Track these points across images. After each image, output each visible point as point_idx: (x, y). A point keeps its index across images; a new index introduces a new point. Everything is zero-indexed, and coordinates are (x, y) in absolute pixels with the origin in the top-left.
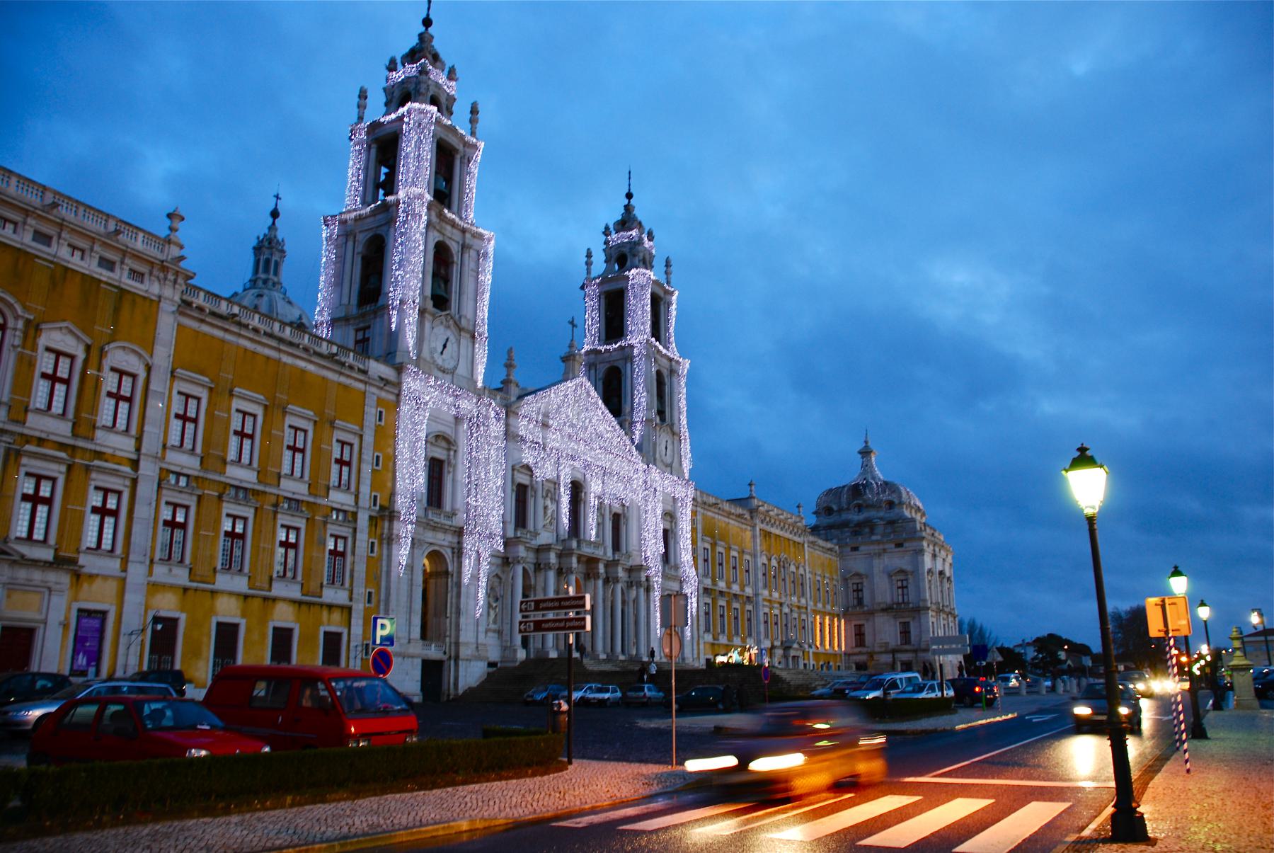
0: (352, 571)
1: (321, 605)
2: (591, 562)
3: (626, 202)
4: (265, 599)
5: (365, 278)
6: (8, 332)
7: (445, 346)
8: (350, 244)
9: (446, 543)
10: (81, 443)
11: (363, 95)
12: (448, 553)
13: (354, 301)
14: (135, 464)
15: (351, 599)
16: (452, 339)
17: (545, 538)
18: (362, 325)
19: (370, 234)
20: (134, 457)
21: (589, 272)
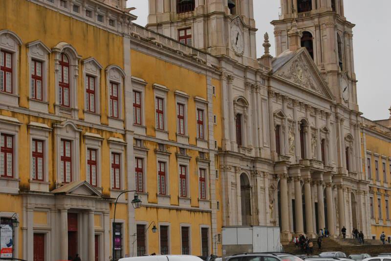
0: (210, 189)
1: (199, 211)
2: (316, 173)
4: (177, 210)
6: (72, 68)
7: (237, 39)
9: (248, 168)
10: (104, 128)
12: (248, 174)
13: (175, 11)
14: (124, 136)
15: (211, 208)
16: (240, 33)
17: (292, 161)
18: (184, 27)
20: (123, 132)
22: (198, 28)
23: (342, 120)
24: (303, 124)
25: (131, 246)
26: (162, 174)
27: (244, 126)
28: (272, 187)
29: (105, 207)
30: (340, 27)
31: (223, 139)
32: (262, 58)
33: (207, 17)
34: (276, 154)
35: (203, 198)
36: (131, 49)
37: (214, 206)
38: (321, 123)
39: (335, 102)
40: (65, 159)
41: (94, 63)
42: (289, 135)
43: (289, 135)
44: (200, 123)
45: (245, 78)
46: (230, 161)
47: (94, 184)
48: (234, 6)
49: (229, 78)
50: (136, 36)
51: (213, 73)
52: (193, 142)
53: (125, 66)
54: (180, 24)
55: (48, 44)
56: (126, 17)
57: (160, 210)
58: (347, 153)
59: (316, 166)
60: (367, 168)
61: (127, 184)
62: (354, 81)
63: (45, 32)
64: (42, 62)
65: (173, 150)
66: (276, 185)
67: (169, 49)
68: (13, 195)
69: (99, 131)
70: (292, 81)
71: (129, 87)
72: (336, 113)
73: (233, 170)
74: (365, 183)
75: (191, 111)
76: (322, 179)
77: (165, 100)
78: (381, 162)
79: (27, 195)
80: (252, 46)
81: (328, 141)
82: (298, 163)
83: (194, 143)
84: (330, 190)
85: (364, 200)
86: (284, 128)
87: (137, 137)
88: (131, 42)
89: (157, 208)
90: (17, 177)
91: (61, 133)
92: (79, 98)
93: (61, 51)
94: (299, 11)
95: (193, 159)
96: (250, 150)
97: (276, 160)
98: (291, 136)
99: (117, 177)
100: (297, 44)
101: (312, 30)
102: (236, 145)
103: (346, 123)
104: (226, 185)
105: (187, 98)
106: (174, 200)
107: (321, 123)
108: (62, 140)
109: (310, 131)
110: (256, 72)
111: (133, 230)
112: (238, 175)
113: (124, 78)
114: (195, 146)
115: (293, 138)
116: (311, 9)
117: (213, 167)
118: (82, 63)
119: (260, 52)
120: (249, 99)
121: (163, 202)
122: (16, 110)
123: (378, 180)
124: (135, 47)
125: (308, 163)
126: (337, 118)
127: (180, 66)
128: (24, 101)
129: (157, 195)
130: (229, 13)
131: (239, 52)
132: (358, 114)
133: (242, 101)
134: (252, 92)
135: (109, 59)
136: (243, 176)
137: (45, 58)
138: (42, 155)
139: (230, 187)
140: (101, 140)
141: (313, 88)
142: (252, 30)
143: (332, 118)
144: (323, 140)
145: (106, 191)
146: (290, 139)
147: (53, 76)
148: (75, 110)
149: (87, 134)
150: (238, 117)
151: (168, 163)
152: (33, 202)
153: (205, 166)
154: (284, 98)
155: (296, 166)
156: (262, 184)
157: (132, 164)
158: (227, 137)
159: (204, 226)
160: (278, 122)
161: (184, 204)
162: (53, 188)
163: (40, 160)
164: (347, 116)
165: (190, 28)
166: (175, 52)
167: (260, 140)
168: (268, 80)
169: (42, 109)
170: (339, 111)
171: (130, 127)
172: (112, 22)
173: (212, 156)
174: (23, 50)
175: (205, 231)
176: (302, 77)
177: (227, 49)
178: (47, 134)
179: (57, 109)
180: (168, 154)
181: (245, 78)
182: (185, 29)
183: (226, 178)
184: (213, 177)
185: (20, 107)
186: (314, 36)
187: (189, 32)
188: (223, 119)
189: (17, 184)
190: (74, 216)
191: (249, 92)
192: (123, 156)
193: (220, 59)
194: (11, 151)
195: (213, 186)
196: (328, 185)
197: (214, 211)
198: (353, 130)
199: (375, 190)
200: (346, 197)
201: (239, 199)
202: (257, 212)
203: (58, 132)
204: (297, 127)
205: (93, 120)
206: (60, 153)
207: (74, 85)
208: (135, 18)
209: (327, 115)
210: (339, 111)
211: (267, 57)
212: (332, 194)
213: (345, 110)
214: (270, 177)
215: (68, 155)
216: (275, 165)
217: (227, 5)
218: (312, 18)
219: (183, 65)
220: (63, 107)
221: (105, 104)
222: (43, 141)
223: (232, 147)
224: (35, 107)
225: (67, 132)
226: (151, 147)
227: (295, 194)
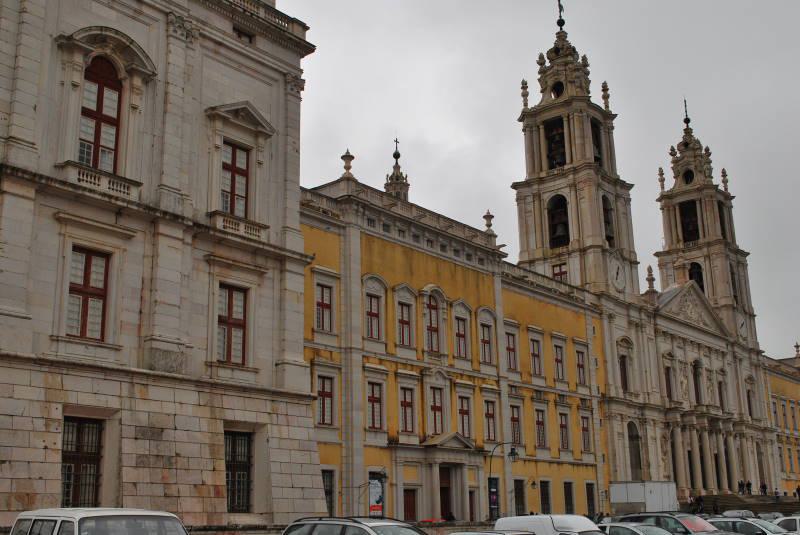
1: (583, 465)
2: (714, 420)
3: (685, 126)
4: (559, 463)
5: (553, 228)
6: (441, 311)
8: (537, 203)
10: (475, 375)
11: (524, 86)
13: (548, 246)
14: (498, 382)
16: (621, 267)
17: (686, 407)
18: (558, 263)
19: (554, 194)
21: (663, 187)
22: (573, 265)
23: (741, 360)
24: (696, 365)
25: (508, 503)
26: (540, 424)
27: (629, 370)
28: (664, 437)
29: (479, 460)
30: (732, 256)
31: (607, 384)
32: (647, 293)
33: (583, 251)
34: (667, 399)
35: (586, 450)
36: (503, 288)
37: (600, 459)
38: (717, 364)
39: (732, 340)
40: (435, 408)
41: (463, 305)
42: (680, 378)
43: (680, 378)
44: (580, 366)
45: (628, 316)
46: (615, 408)
47: (467, 435)
48: (612, 238)
49: (611, 317)
50: (507, 275)
51: (592, 311)
52: (573, 388)
53: (497, 307)
54: (553, 260)
55: (415, 289)
56: (496, 255)
57: (539, 464)
58: (749, 397)
59: (713, 412)
60: (773, 414)
61: (502, 434)
62: (752, 316)
63: (412, 274)
64: (409, 306)
65: (551, 397)
66: (669, 435)
67: (543, 287)
68: (381, 448)
69: (470, 377)
70: (681, 317)
71: (502, 330)
72: (734, 352)
73: (619, 418)
74: (772, 431)
75: (570, 352)
76: (721, 427)
77: (541, 343)
78: (789, 406)
79: (396, 449)
80: (634, 281)
81: (726, 384)
82: (693, 409)
83: (574, 389)
84: (731, 439)
85: (772, 451)
86: (675, 370)
87: (511, 383)
88: (503, 281)
89: (536, 461)
90: (385, 429)
91: (430, 381)
92: (448, 343)
93: (429, 293)
94: (686, 240)
95: (574, 407)
96: (637, 396)
97: (668, 406)
98: (683, 378)
99: (491, 428)
100: (684, 275)
101: (700, 261)
102: (621, 391)
103: (746, 363)
104: (612, 435)
105: (565, 340)
106: (555, 451)
107: (717, 364)
108: (431, 388)
109: (704, 373)
110: (640, 309)
111: (511, 486)
112: (625, 424)
113: (495, 320)
114: (575, 392)
115: (685, 381)
116: (698, 238)
117: (597, 415)
118: (451, 305)
119: (644, 287)
120: (633, 338)
121: (542, 455)
122: (383, 357)
123: (786, 427)
124: (506, 286)
125: (705, 409)
126: (735, 357)
127: (556, 305)
128: (391, 349)
129: (535, 447)
130: (607, 246)
131: (620, 288)
132: (759, 353)
133: (626, 341)
134: (637, 331)
135: (478, 300)
136: (631, 426)
137: (412, 301)
138: (410, 405)
139: (616, 437)
140: (473, 388)
141: (705, 324)
142: (634, 263)
143: (729, 358)
144: (720, 383)
145: (480, 443)
146: (683, 383)
147: (421, 321)
148: (444, 355)
149: (458, 381)
150: (623, 359)
151: (546, 412)
152: (402, 455)
153: (587, 414)
154: (673, 337)
155: (691, 413)
156: (653, 434)
157: (507, 413)
158: (611, 381)
159: (590, 482)
160: (668, 364)
161: (566, 457)
162: (423, 439)
163: (409, 410)
164: (746, 355)
165: (565, 264)
166: (550, 290)
167: (647, 383)
168: (655, 317)
169: (411, 355)
170: (736, 349)
171: (503, 372)
172: (481, 261)
173: (595, 402)
174: (390, 294)
175: (590, 487)
176: (693, 313)
177: (607, 285)
178: (416, 383)
179: (426, 355)
180: (547, 402)
181: (628, 316)
182: (560, 266)
183: (612, 428)
184: (597, 426)
185: (388, 354)
186: (703, 267)
187: (564, 269)
188: (605, 362)
189: (386, 436)
190: (447, 470)
191: (633, 331)
192: (497, 404)
193: (599, 296)
194: (379, 400)
195: (597, 435)
196: (728, 433)
197: (600, 465)
198: (754, 371)
199: (784, 439)
200: (749, 447)
201: (628, 450)
202: (649, 466)
203: (427, 380)
204: (690, 368)
205: (461, 365)
206: (429, 402)
207: (443, 327)
208: (506, 255)
209: (724, 354)
210: (736, 349)
211: (652, 292)
212: (733, 444)
213: (744, 348)
214: (662, 426)
215: (438, 404)
216: (667, 411)
217: (604, 237)
218: (700, 248)
219: (560, 304)
220: (431, 352)
221: (476, 349)
222: (411, 390)
223: (617, 393)
224: (402, 353)
225: (437, 379)
226: (527, 395)
227: (691, 444)
